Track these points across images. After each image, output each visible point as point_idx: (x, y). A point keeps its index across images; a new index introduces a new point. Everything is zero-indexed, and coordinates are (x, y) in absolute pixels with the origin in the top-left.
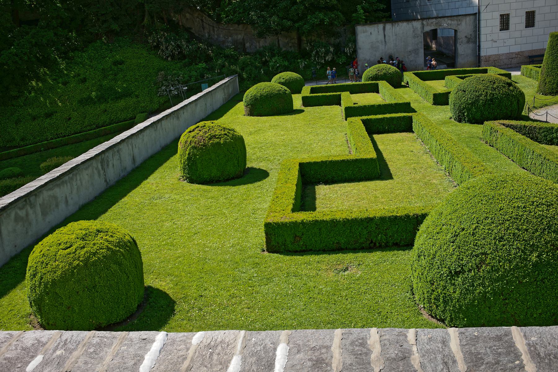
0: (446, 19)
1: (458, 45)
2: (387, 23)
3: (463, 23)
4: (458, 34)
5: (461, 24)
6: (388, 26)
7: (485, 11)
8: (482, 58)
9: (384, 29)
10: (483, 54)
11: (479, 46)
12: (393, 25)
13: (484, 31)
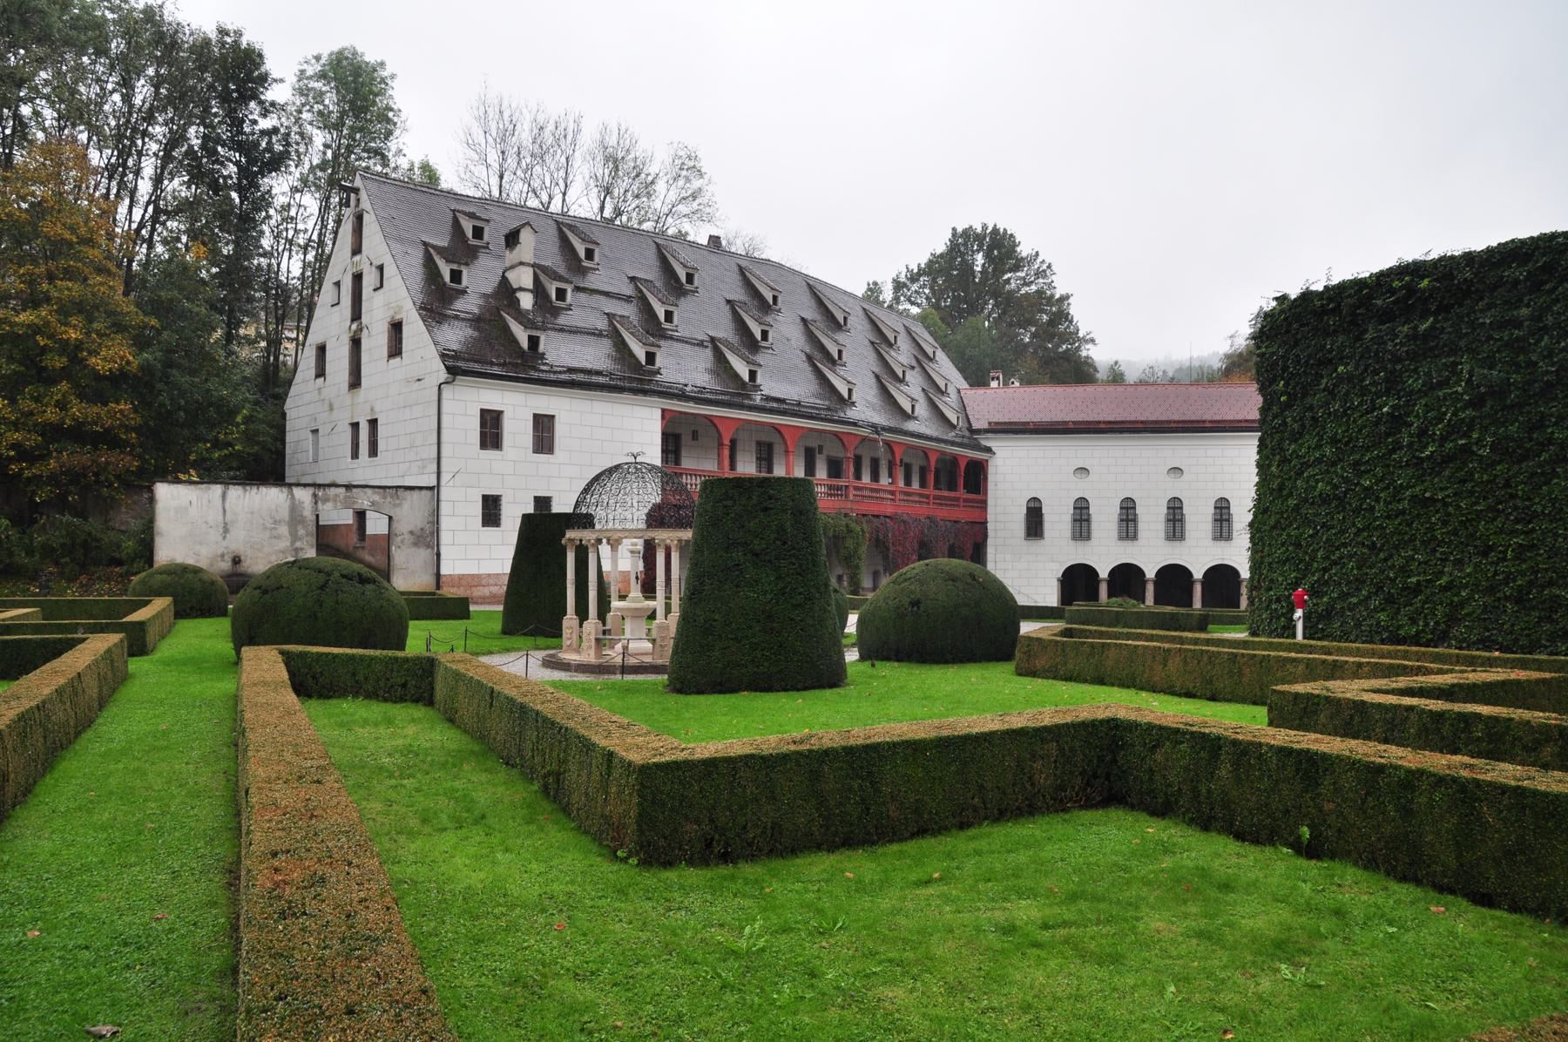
0: (369, 491)
1: (394, 548)
2: (234, 484)
3: (406, 506)
4: (395, 525)
5: (400, 505)
6: (235, 492)
7: (451, 483)
8: (443, 580)
9: (224, 496)
10: (443, 571)
11: (438, 555)
12: (245, 491)
13: (445, 523)
